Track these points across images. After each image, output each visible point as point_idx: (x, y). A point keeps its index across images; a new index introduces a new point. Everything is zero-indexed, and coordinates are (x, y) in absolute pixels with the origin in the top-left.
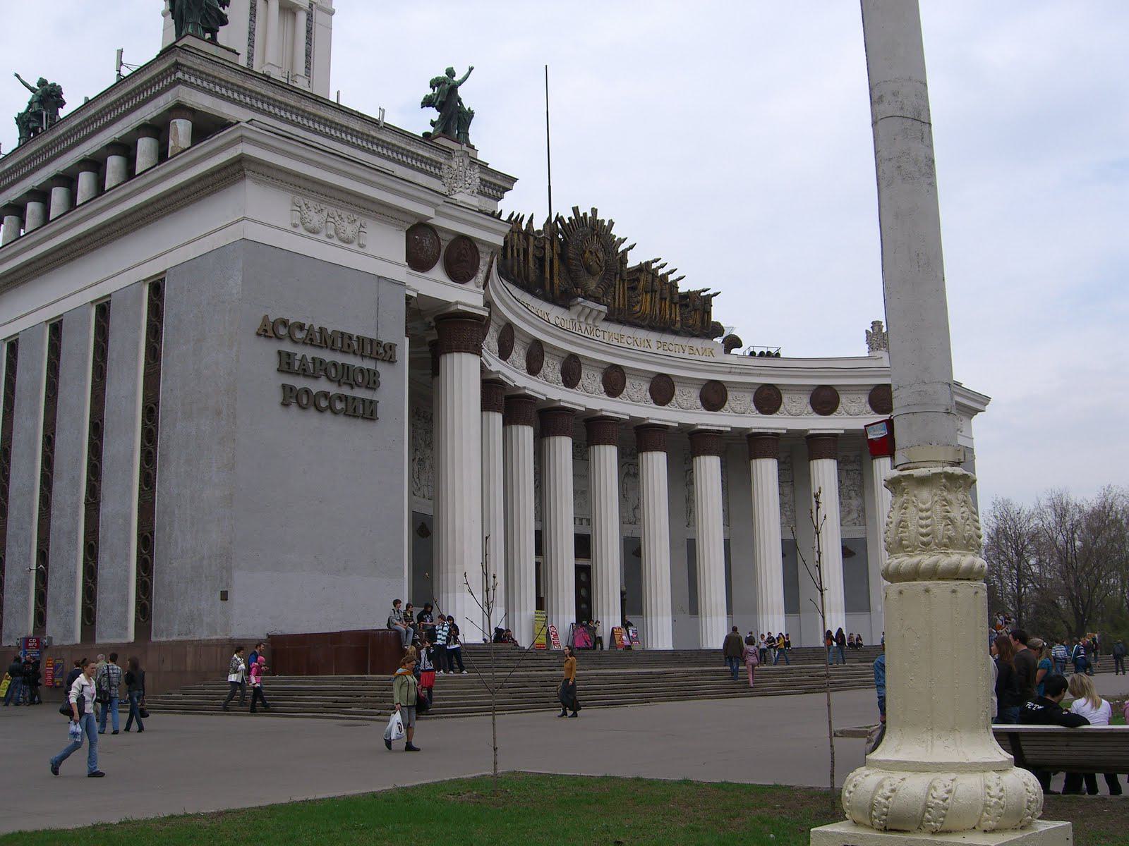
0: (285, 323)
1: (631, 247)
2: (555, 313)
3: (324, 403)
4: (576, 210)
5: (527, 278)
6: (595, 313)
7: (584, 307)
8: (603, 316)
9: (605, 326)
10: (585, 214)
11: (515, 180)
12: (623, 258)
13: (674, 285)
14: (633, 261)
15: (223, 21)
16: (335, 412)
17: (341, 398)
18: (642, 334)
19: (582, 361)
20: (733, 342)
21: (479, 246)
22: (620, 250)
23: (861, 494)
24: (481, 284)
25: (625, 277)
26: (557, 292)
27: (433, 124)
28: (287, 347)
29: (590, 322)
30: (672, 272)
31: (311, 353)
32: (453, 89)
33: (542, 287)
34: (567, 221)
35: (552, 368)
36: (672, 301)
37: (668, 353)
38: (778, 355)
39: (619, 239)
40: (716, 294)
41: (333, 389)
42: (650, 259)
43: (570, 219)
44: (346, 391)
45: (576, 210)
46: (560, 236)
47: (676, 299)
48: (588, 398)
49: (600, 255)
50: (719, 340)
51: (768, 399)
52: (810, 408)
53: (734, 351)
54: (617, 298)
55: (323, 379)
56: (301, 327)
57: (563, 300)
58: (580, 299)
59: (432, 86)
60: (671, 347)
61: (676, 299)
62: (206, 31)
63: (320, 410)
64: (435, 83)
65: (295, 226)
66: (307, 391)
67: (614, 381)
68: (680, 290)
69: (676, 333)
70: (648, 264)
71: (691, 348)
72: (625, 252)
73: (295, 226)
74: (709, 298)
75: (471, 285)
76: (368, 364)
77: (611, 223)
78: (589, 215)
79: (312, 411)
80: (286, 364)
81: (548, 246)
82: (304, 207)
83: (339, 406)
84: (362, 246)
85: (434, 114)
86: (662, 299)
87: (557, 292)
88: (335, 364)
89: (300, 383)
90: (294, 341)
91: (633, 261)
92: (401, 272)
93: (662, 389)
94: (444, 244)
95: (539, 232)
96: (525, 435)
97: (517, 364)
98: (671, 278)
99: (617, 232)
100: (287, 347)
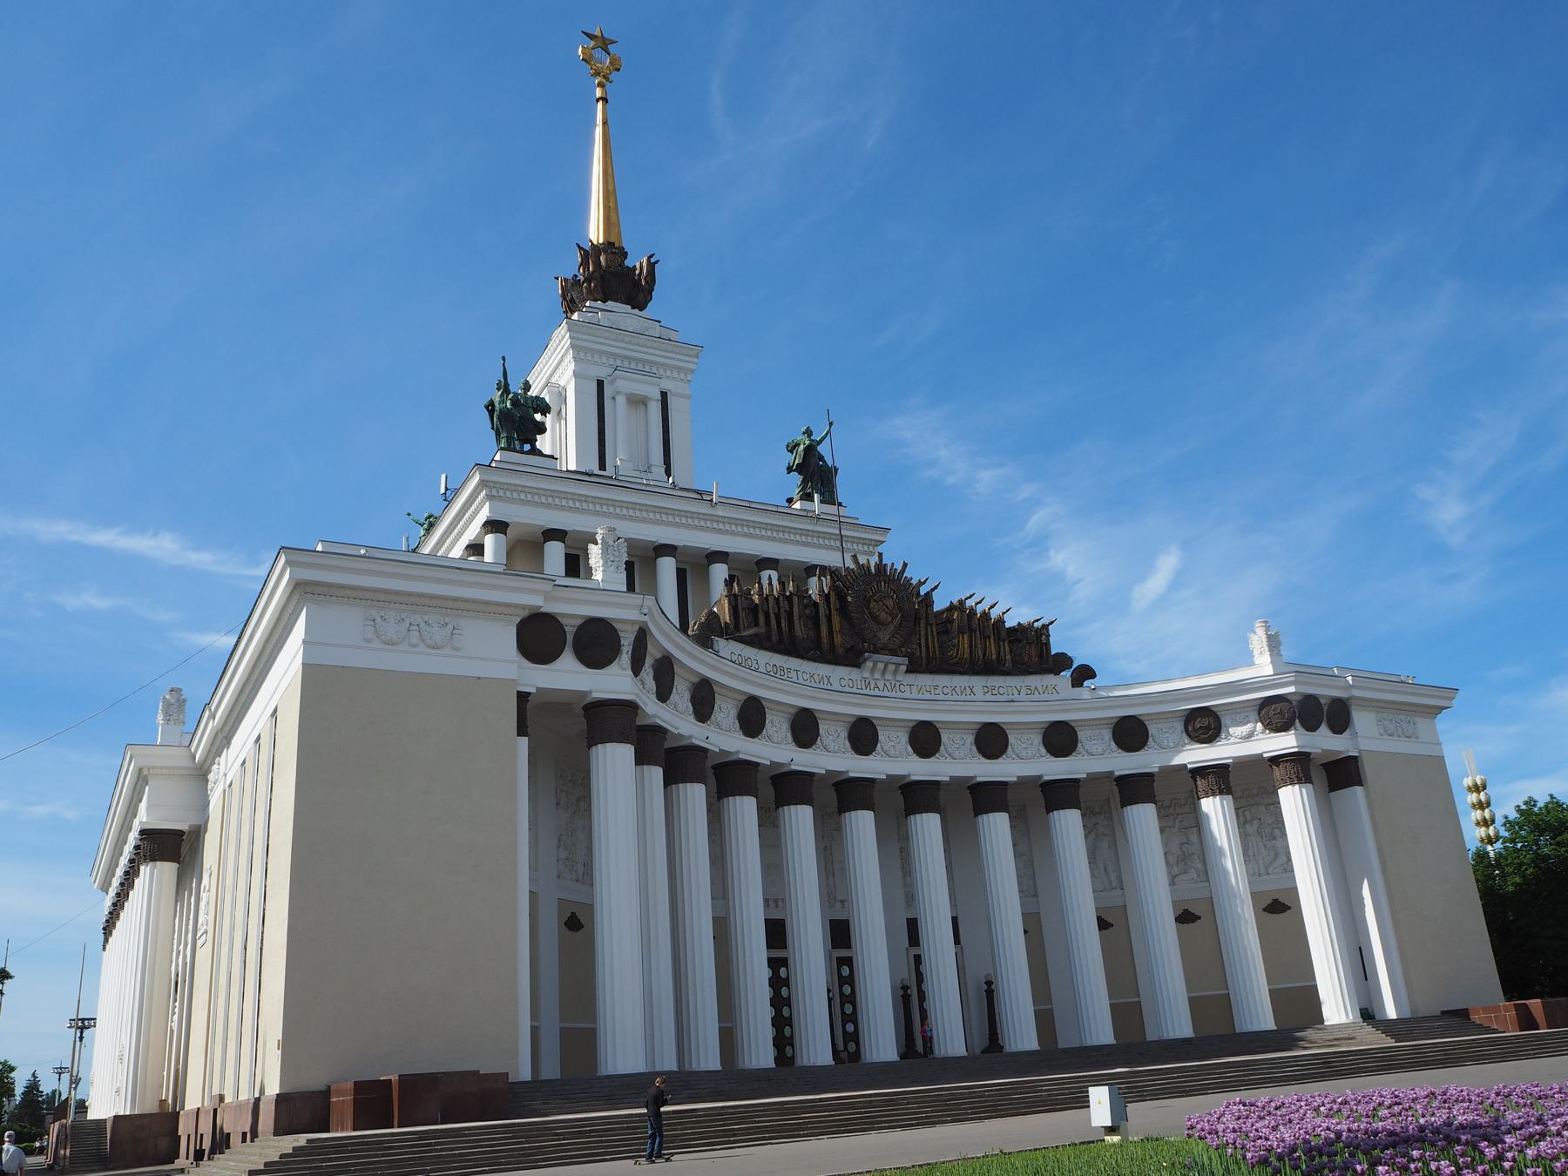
6: (892, 667)
12: (928, 599)
13: (1001, 621)
18: (960, 681)
20: (1084, 674)
25: (933, 621)
26: (840, 651)
29: (888, 676)
47: (1004, 633)
50: (1067, 674)
51: (1130, 733)
57: (852, 659)
62: (523, 442)
64: (792, 448)
65: (367, 641)
68: (1008, 625)
71: (1028, 688)
72: (929, 595)
75: (613, 668)
82: (378, 620)
84: (456, 649)
87: (840, 651)
98: (994, 614)
99: (913, 574)
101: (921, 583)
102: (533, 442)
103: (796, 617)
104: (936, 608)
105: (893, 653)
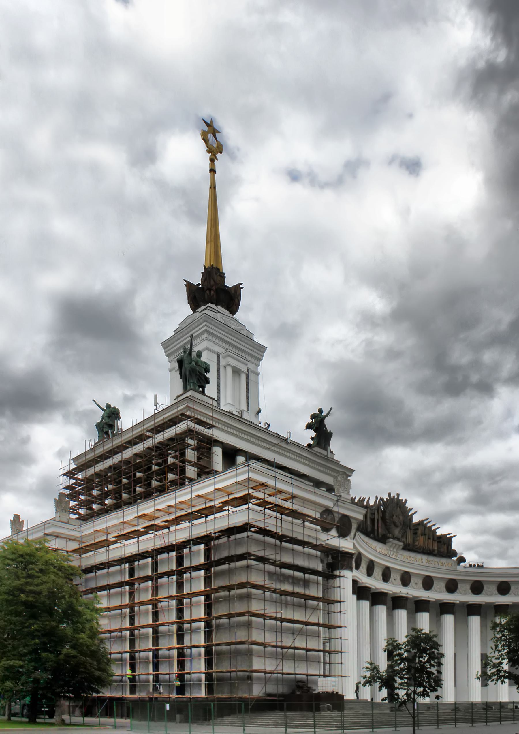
1: (415, 513)
2: (379, 546)
4: (389, 494)
5: (367, 529)
7: (393, 543)
8: (401, 547)
10: (394, 497)
11: (353, 471)
12: (411, 519)
13: (434, 531)
14: (416, 519)
15: (207, 381)
18: (419, 556)
21: (352, 520)
22: (409, 514)
24: (352, 538)
26: (380, 536)
27: (312, 439)
32: (322, 420)
33: (374, 533)
34: (385, 500)
36: (434, 540)
37: (431, 565)
38: (482, 566)
39: (410, 509)
40: (454, 536)
42: (424, 519)
43: (387, 499)
45: (389, 494)
46: (382, 508)
47: (436, 539)
49: (401, 517)
50: (455, 559)
52: (497, 592)
53: (462, 564)
57: (383, 540)
58: (391, 540)
59: (312, 418)
60: (432, 562)
61: (436, 539)
68: (437, 534)
69: (435, 555)
72: (412, 515)
74: (451, 537)
77: (406, 501)
78: (396, 497)
81: (376, 513)
85: (313, 434)
86: (429, 538)
87: (380, 536)
91: (416, 519)
93: (428, 583)
94: (337, 519)
95: (372, 506)
99: (408, 505)
101: (411, 510)
102: (203, 388)
104: (413, 522)
105: (399, 540)
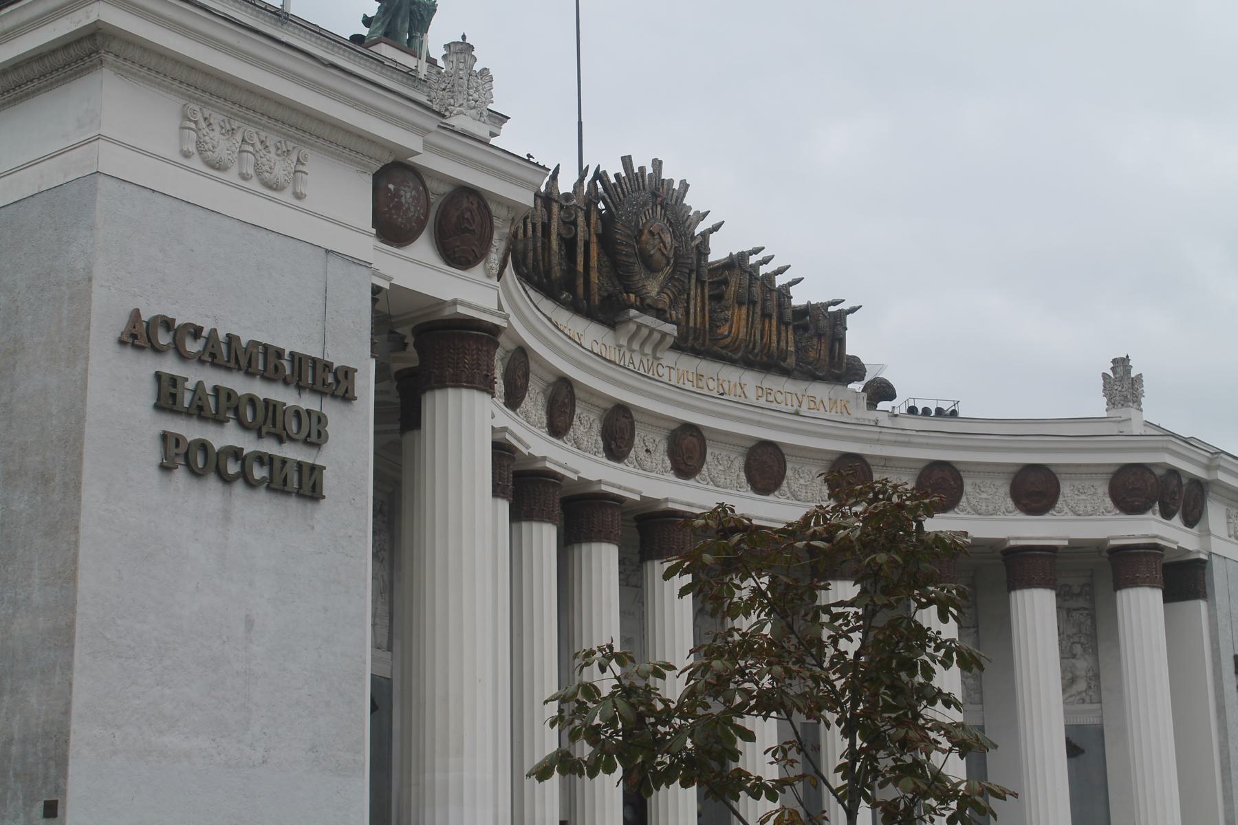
0: (168, 324)
1: (716, 228)
2: (591, 334)
3: (233, 468)
4: (627, 161)
5: (548, 272)
6: (657, 336)
7: (640, 326)
8: (670, 341)
9: (669, 358)
10: (642, 169)
12: (702, 249)
14: (718, 251)
16: (251, 484)
17: (261, 459)
18: (732, 375)
19: (636, 416)
20: (881, 391)
21: (493, 207)
22: (697, 232)
23: (1092, 648)
24: (495, 272)
25: (706, 278)
27: (367, 21)
28: (170, 366)
30: (781, 271)
31: (212, 378)
33: (571, 288)
34: (613, 180)
35: (587, 425)
36: (781, 320)
37: (774, 406)
38: (954, 413)
39: (697, 213)
40: (853, 310)
41: (249, 444)
42: (747, 248)
43: (617, 176)
44: (269, 447)
46: (601, 206)
48: (644, 480)
49: (668, 238)
50: (857, 386)
52: (1010, 503)
53: (883, 405)
54: (692, 311)
55: (231, 425)
56: (196, 332)
57: (607, 313)
58: (633, 312)
60: (780, 398)
63: (226, 480)
66: (204, 446)
67: (687, 449)
69: (786, 373)
70: (743, 256)
72: (705, 235)
73: (186, 155)
74: (840, 318)
75: (477, 272)
76: (308, 402)
77: (685, 186)
78: (649, 170)
79: (212, 483)
80: (168, 396)
81: (581, 220)
82: (203, 124)
83: (259, 473)
86: (766, 315)
87: (596, 299)
88: (252, 400)
89: (191, 431)
90: (183, 356)
92: (366, 246)
94: (436, 202)
95: (567, 196)
96: (545, 536)
97: (533, 418)
98: (780, 281)
99: (693, 201)
100: (170, 366)
103: (554, 237)
104: (712, 258)
105: (660, 314)
